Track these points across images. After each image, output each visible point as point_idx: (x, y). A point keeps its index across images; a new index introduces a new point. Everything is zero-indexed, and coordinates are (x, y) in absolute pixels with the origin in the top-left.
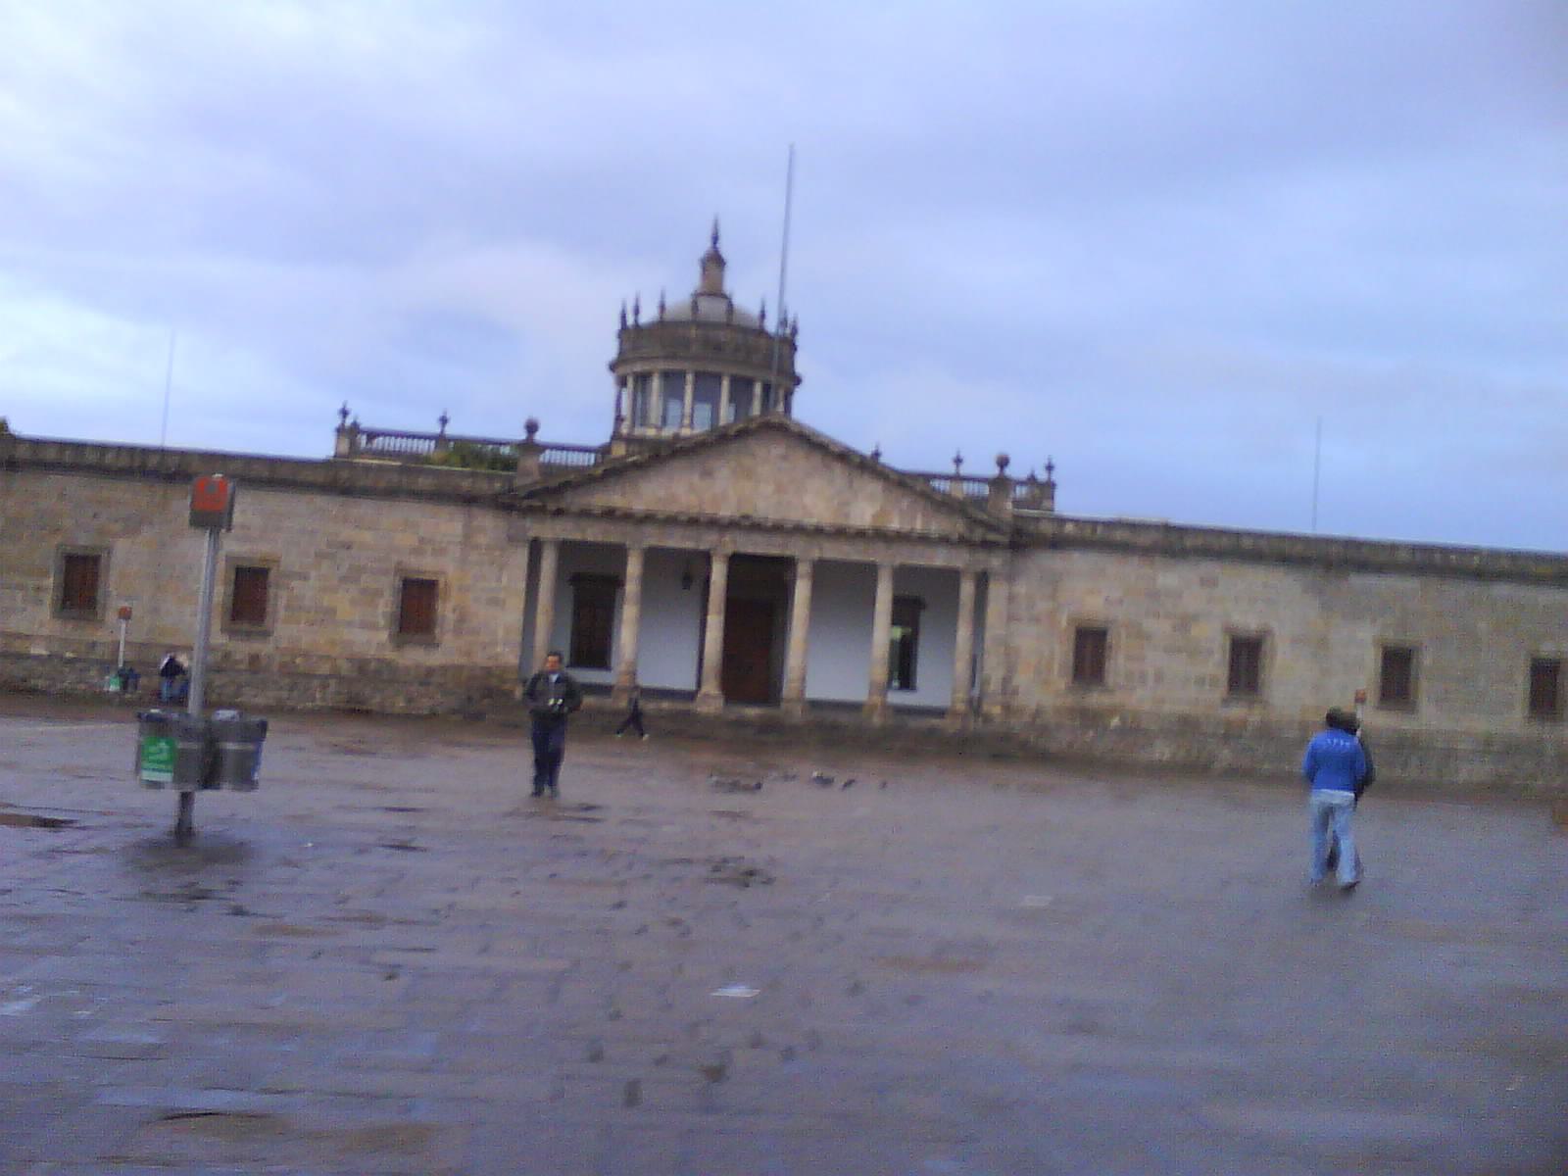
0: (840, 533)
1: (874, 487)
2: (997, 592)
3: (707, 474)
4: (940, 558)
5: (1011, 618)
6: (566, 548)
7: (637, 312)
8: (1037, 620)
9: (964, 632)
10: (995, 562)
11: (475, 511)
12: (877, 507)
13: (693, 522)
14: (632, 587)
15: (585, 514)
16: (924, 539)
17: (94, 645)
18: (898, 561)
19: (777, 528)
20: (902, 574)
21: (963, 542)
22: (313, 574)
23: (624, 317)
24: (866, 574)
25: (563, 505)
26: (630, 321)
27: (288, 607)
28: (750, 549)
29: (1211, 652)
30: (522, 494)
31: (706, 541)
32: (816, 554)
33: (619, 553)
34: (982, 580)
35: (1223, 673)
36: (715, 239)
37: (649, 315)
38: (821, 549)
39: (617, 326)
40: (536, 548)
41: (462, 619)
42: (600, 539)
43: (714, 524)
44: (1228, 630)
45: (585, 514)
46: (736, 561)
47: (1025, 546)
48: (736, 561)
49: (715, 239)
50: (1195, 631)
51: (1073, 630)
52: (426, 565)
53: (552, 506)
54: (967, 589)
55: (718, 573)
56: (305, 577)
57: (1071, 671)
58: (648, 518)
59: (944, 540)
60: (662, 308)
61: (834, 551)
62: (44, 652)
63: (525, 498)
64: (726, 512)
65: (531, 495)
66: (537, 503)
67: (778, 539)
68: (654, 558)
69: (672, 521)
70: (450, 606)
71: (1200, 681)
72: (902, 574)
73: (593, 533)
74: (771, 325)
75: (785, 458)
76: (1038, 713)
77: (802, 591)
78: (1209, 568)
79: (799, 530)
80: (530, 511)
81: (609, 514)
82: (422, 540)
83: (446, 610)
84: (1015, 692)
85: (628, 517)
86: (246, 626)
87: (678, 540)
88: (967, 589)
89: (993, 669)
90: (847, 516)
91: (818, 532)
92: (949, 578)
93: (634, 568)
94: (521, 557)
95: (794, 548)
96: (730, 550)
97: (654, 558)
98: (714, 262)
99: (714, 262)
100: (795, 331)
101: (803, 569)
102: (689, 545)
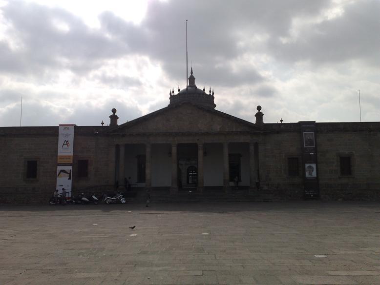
4: (242, 139)
23: (171, 94)
26: (172, 94)
34: (256, 145)
37: (176, 93)
39: (170, 96)
46: (179, 146)
48: (179, 146)
54: (252, 148)
55: (174, 150)
60: (179, 90)
74: (207, 92)
77: (200, 153)
88: (252, 148)
99: (192, 80)
100: (213, 93)
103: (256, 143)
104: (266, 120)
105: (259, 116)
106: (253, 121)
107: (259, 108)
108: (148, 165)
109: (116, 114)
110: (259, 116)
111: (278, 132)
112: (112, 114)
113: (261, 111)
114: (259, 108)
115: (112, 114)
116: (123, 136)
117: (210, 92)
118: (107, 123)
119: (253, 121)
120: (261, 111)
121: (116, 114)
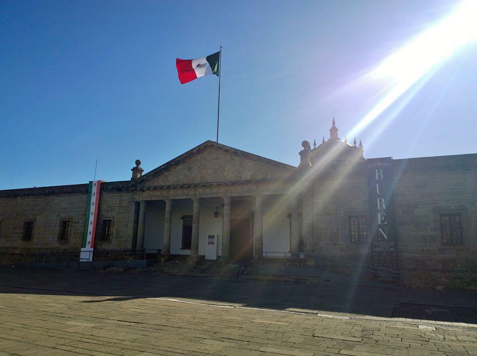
17: (29, 249)
22: (81, 221)
36: (334, 123)
40: (138, 204)
49: (334, 123)
56: (78, 223)
62: (19, 252)
63: (131, 187)
70: (114, 228)
75: (216, 159)
82: (108, 206)
83: (113, 230)
90: (241, 178)
112: (135, 166)
115: (135, 166)
121: (141, 166)
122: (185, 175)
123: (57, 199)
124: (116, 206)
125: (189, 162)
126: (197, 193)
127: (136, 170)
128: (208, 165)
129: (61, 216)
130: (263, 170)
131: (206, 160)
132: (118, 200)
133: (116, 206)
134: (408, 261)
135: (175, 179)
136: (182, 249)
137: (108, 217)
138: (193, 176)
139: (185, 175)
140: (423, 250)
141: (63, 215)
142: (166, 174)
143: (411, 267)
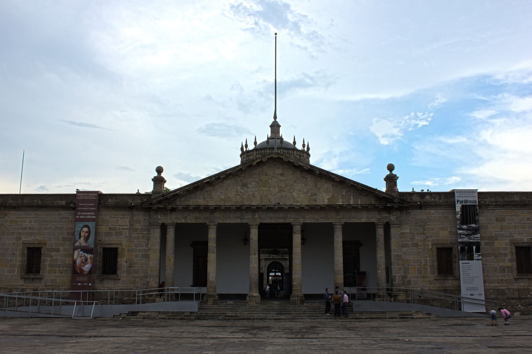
0: (312, 209)
1: (328, 185)
2: (394, 231)
3: (244, 185)
4: (364, 218)
5: (403, 246)
6: (179, 227)
7: (246, 146)
8: (416, 245)
9: (381, 254)
10: (393, 218)
11: (135, 212)
12: (331, 194)
13: (239, 209)
14: (212, 244)
15: (186, 209)
16: (355, 208)
18: (344, 221)
19: (280, 209)
20: (347, 227)
21: (374, 208)
22: (61, 248)
23: (242, 149)
24: (329, 228)
25: (174, 206)
26: (245, 149)
27: (50, 265)
28: (268, 221)
29: (506, 255)
30: (155, 201)
31: (247, 219)
32: (302, 221)
33: (204, 228)
34: (387, 227)
35: (514, 264)
36: (275, 117)
37: (251, 147)
38: (304, 218)
39: (240, 152)
40: (164, 228)
41: (130, 266)
42: (194, 221)
43: (249, 209)
44: (512, 242)
45: (186, 209)
46: (262, 227)
47: (407, 208)
48: (262, 227)
49: (275, 117)
50: (496, 244)
51: (435, 250)
52: (112, 240)
53: (169, 207)
54: (380, 232)
56: (58, 250)
57: (436, 271)
58: (217, 209)
59: (365, 208)
60: (255, 143)
61: (310, 218)
63: (156, 204)
64: (255, 203)
65: (159, 202)
66: (161, 206)
67: (281, 215)
68: (222, 229)
69: (228, 209)
70: (124, 259)
71: (503, 269)
72: (347, 227)
73: (191, 219)
74: (299, 147)
75: (282, 175)
76: (422, 292)
77: (297, 239)
78: (499, 212)
79: (291, 209)
80: (158, 210)
81: (197, 208)
82: (110, 228)
83: (122, 262)
84: (409, 282)
85: (206, 208)
86: (32, 276)
87: (233, 219)
88: (380, 232)
89: (397, 273)
90: (315, 201)
91: (301, 209)
92: (371, 227)
93: (212, 234)
94: (156, 233)
95: (290, 218)
96: (258, 221)
97: (222, 229)
98: (275, 127)
100: (308, 149)
101: (297, 229)
102: (238, 221)
103: (387, 223)
104: (402, 187)
105: (391, 180)
106: (383, 188)
107: (391, 168)
108: (212, 257)
109: (163, 175)
110: (391, 180)
111: (420, 207)
113: (394, 172)
114: (391, 168)
116: (173, 210)
117: (304, 146)
118: (148, 188)
119: (383, 188)
120: (394, 172)
121: (163, 175)
122: (237, 191)
123: (13, 215)
124: (125, 229)
125: (243, 175)
126: (257, 216)
127: (159, 181)
128: (270, 181)
129: (23, 239)
130: (344, 193)
131: (267, 175)
132: (128, 220)
133: (125, 229)
134: (490, 291)
135: (223, 197)
136: (192, 286)
137: (111, 244)
138: (250, 194)
139: (237, 191)
140: (502, 280)
141: (30, 239)
142: (210, 188)
143: (493, 297)
